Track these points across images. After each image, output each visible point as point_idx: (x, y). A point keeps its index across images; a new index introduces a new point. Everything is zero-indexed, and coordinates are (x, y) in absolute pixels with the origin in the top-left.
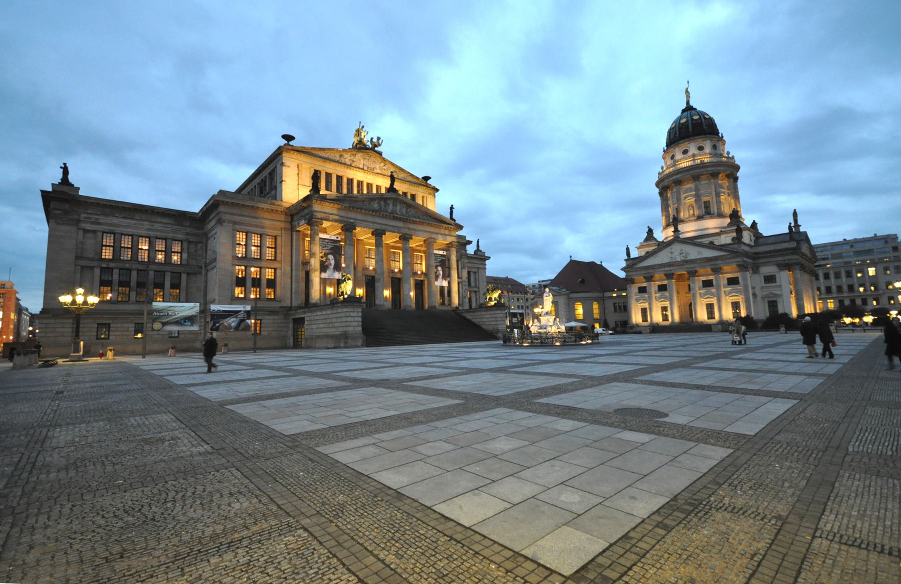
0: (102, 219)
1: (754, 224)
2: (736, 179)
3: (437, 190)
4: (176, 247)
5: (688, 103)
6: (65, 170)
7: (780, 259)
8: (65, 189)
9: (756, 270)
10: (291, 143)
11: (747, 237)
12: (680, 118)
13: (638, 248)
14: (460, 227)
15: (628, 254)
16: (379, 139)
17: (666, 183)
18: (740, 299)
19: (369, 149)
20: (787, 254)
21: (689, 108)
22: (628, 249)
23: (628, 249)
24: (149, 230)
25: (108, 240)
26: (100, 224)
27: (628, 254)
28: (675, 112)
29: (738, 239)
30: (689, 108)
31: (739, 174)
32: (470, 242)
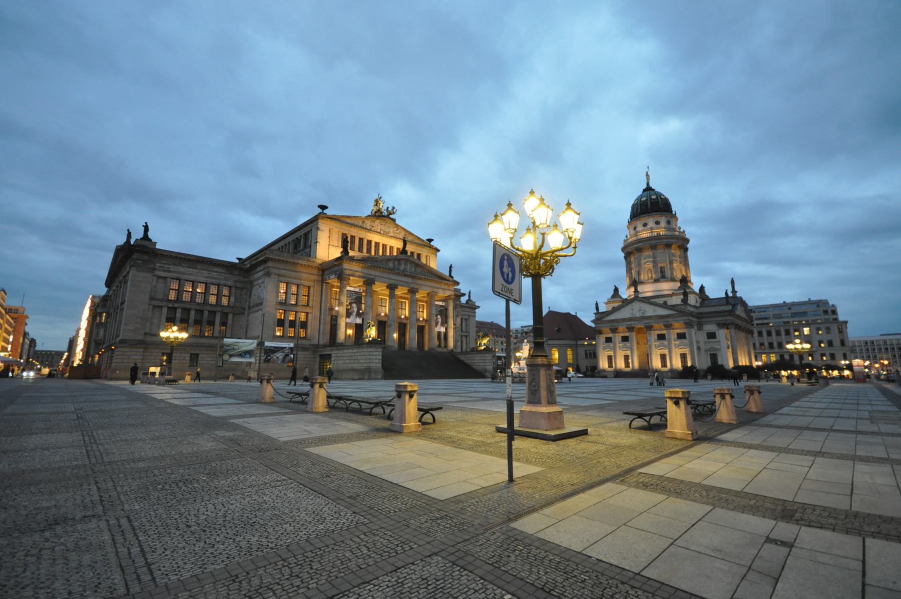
0: (172, 268)
1: (702, 288)
2: (686, 250)
3: (438, 251)
4: (226, 291)
5: (648, 184)
6: (146, 228)
7: (719, 319)
8: (146, 243)
9: (700, 327)
10: (325, 211)
11: (692, 300)
12: (641, 196)
13: (606, 303)
14: (458, 283)
15: (597, 308)
16: (394, 208)
17: (629, 249)
18: (687, 351)
19: (384, 216)
20: (724, 316)
21: (648, 189)
22: (597, 304)
23: (597, 304)
24: (207, 277)
25: (175, 285)
26: (170, 272)
27: (597, 308)
28: (634, 193)
29: (685, 301)
30: (648, 189)
31: (688, 246)
32: (464, 295)
